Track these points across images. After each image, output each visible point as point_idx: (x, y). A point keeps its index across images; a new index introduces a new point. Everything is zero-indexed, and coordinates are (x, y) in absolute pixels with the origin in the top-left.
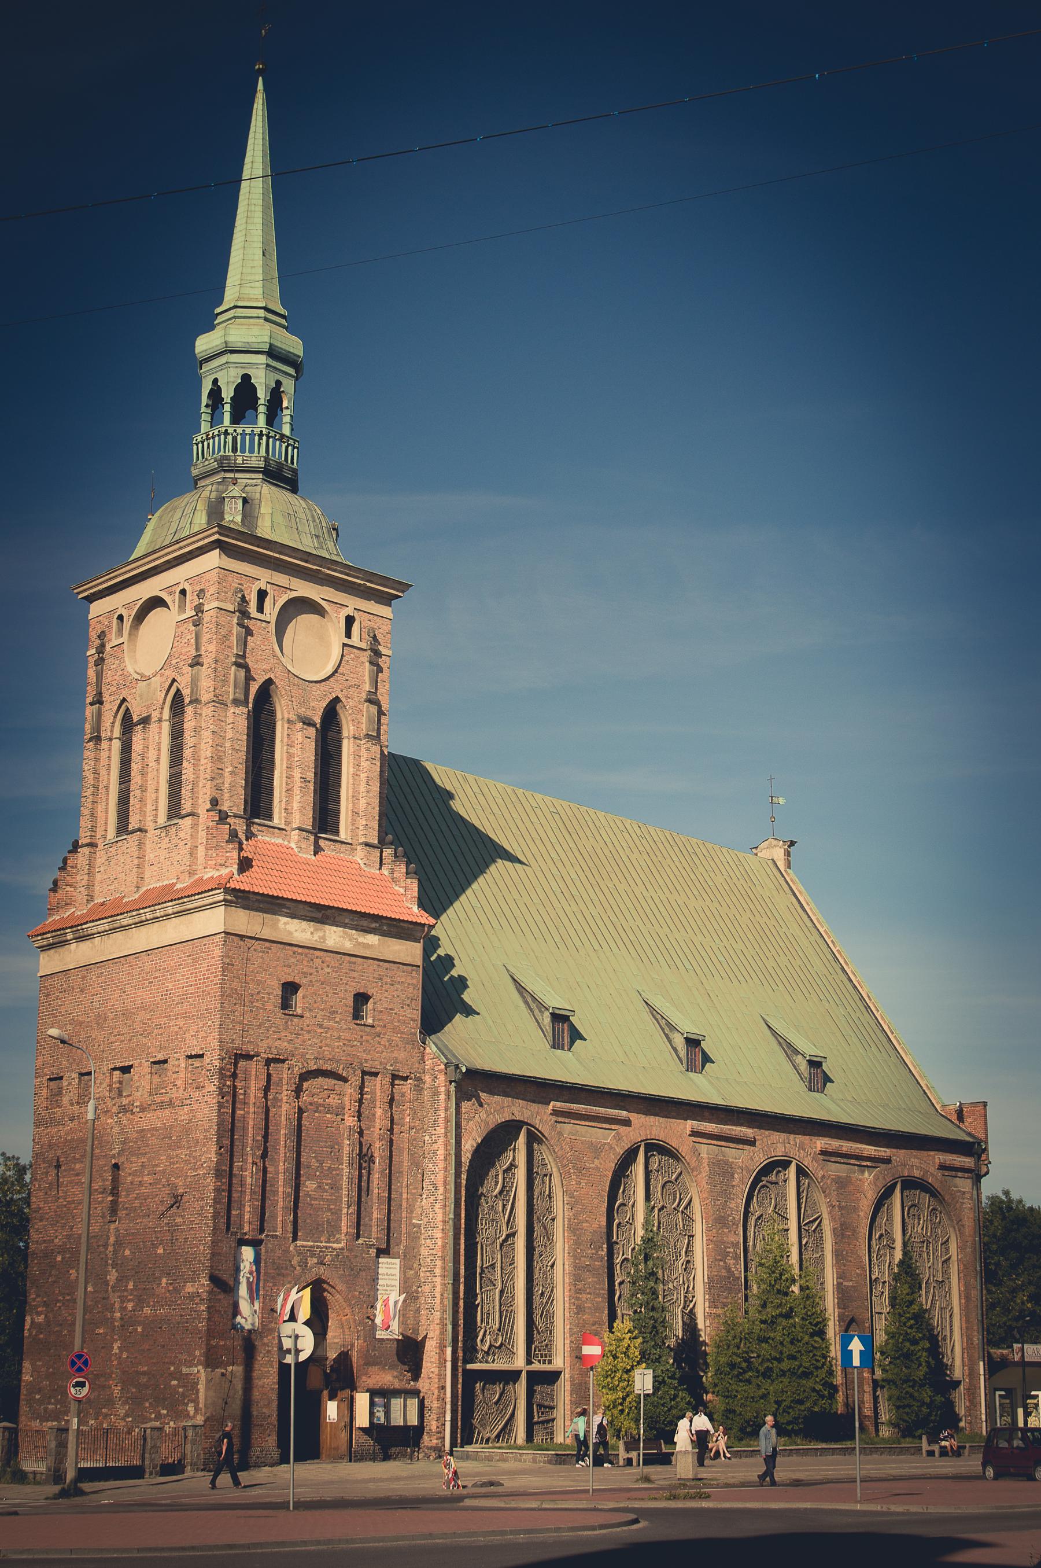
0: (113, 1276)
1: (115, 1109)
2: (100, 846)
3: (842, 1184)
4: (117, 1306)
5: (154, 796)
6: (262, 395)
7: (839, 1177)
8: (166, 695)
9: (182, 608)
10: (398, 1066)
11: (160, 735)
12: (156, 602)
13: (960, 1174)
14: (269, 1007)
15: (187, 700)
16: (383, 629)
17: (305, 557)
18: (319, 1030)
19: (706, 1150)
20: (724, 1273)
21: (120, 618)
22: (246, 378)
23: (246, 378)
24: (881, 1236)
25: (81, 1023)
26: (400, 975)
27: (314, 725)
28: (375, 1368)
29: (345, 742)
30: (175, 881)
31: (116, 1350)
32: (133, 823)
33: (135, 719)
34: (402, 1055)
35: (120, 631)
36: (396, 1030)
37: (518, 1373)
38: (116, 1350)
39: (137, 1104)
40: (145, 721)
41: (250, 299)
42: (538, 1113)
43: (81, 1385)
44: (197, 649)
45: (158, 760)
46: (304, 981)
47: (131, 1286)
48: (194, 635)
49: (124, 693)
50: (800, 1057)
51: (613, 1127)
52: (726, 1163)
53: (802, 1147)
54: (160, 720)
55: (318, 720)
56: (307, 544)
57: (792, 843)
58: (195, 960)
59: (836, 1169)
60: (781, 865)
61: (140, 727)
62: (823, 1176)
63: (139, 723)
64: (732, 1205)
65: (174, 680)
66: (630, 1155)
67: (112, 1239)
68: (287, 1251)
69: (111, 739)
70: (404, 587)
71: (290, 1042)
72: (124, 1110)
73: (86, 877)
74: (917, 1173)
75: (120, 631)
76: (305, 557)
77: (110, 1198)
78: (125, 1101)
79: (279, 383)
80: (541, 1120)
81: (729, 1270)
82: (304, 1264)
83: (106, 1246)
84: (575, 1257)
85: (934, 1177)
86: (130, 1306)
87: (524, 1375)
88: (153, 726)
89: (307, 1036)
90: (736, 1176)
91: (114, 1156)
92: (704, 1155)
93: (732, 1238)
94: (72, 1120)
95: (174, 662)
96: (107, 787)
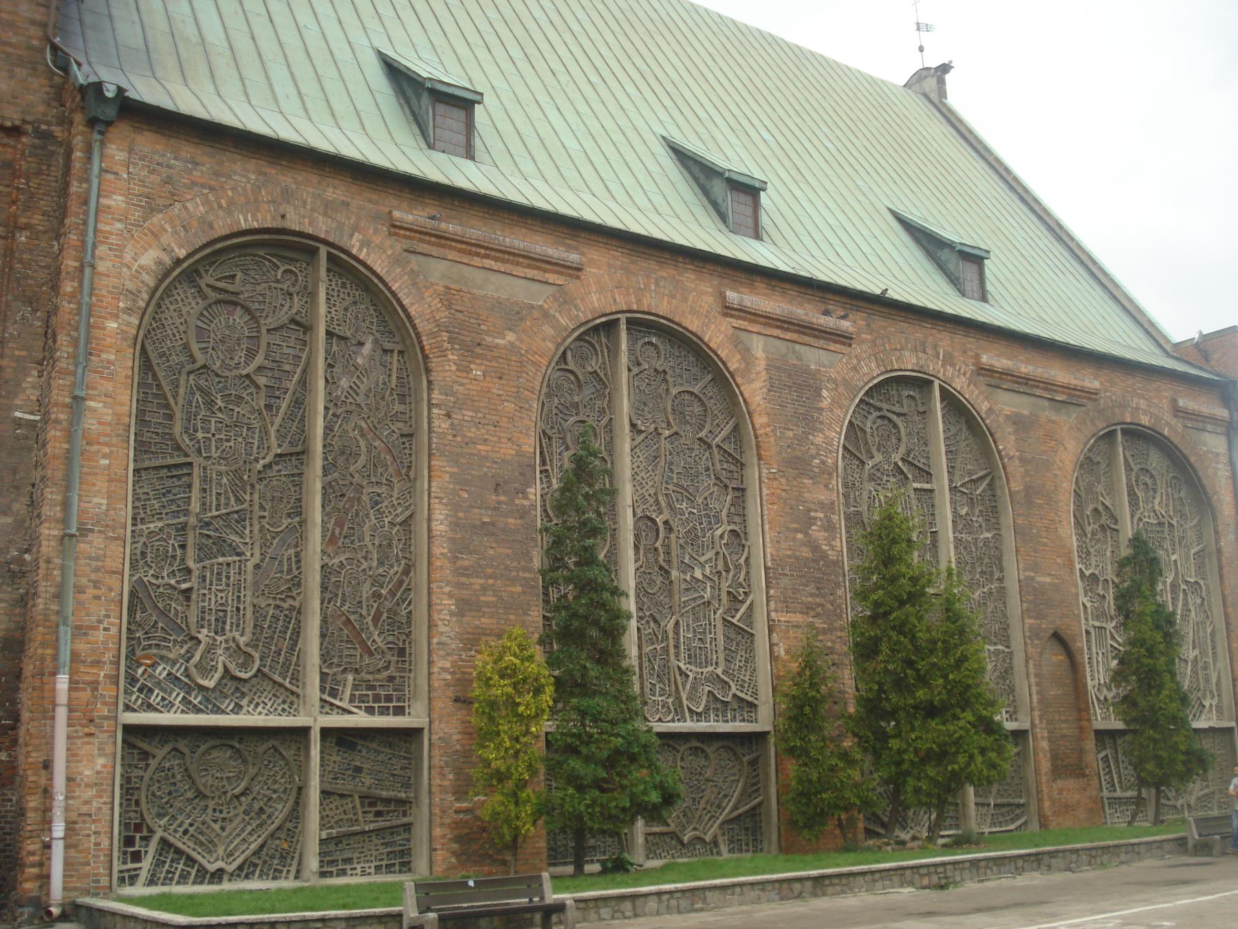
3: (1020, 424)
7: (1017, 414)
13: (1209, 427)
20: (806, 553)
24: (1096, 510)
37: (304, 731)
42: (356, 228)
50: (946, 251)
51: (551, 278)
52: (807, 371)
53: (948, 360)
57: (945, 68)
60: (934, 96)
62: (990, 410)
64: (819, 439)
74: (1145, 420)
80: (366, 243)
81: (815, 548)
84: (455, 507)
85: (1170, 428)
87: (315, 736)
90: (825, 393)
92: (760, 354)
93: (823, 496)
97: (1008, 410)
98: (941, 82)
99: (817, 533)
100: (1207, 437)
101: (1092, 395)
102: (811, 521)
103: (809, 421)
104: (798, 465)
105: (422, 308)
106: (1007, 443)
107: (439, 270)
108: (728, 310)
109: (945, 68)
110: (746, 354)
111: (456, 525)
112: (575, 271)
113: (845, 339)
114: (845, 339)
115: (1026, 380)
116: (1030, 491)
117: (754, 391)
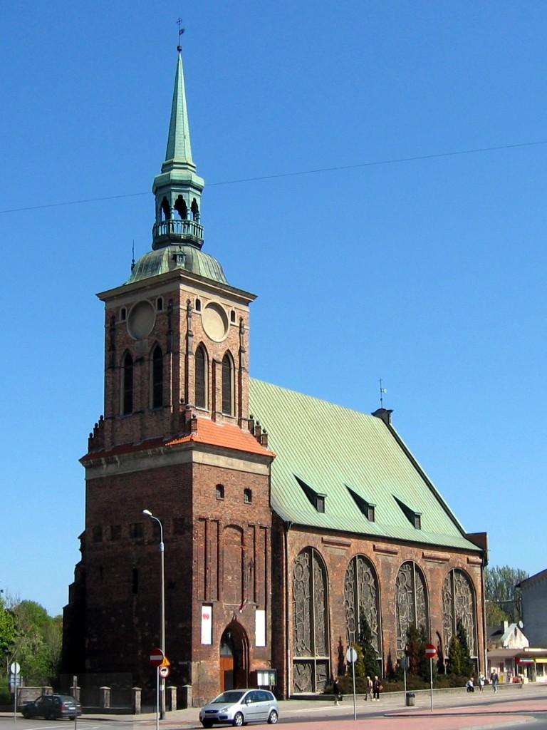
0: (136, 620)
1: (133, 543)
2: (118, 418)
3: (431, 571)
4: (140, 633)
5: (147, 396)
6: (189, 205)
8: (152, 349)
9: (160, 308)
10: (262, 523)
11: (149, 367)
12: (143, 304)
14: (211, 496)
15: (164, 352)
16: (245, 316)
17: (215, 283)
18: (232, 506)
19: (381, 557)
20: (388, 613)
21: (124, 311)
22: (180, 197)
23: (180, 197)
25: (112, 502)
26: (261, 479)
27: (219, 363)
28: (257, 660)
29: (232, 371)
30: (162, 436)
31: (140, 653)
32: (136, 407)
33: (134, 359)
34: (263, 517)
35: (124, 317)
36: (261, 506)
38: (140, 653)
39: (146, 541)
40: (141, 360)
41: (180, 159)
43: (165, 670)
44: (170, 326)
45: (148, 379)
46: (224, 484)
47: (147, 624)
48: (167, 320)
49: (127, 346)
54: (149, 360)
55: (221, 360)
56: (214, 277)
57: (391, 411)
58: (177, 475)
59: (430, 565)
61: (138, 364)
63: (137, 361)
65: (156, 342)
66: (354, 559)
67: (135, 603)
68: (221, 608)
69: (120, 368)
70: (254, 297)
71: (220, 512)
72: (141, 543)
73: (110, 434)
74: (460, 565)
75: (124, 317)
76: (215, 283)
77: (132, 585)
78: (139, 539)
79: (195, 199)
81: (390, 612)
82: (228, 614)
83: (131, 606)
84: (333, 608)
85: (467, 567)
86: (147, 634)
88: (146, 363)
89: (227, 509)
91: (134, 565)
92: (380, 560)
94: (108, 547)
95: (156, 333)
96: (119, 391)
97: (428, 567)
98: (389, 416)
99: (390, 607)
100: (476, 569)
101: (448, 560)
102: (389, 605)
103: (389, 577)
104: (387, 589)
105: (327, 560)
106: (428, 578)
107: (330, 549)
108: (375, 549)
109: (391, 411)
110: (377, 560)
111: (333, 613)
112: (349, 546)
113: (396, 553)
114: (396, 553)
115: (434, 558)
116: (433, 591)
117: (379, 571)
